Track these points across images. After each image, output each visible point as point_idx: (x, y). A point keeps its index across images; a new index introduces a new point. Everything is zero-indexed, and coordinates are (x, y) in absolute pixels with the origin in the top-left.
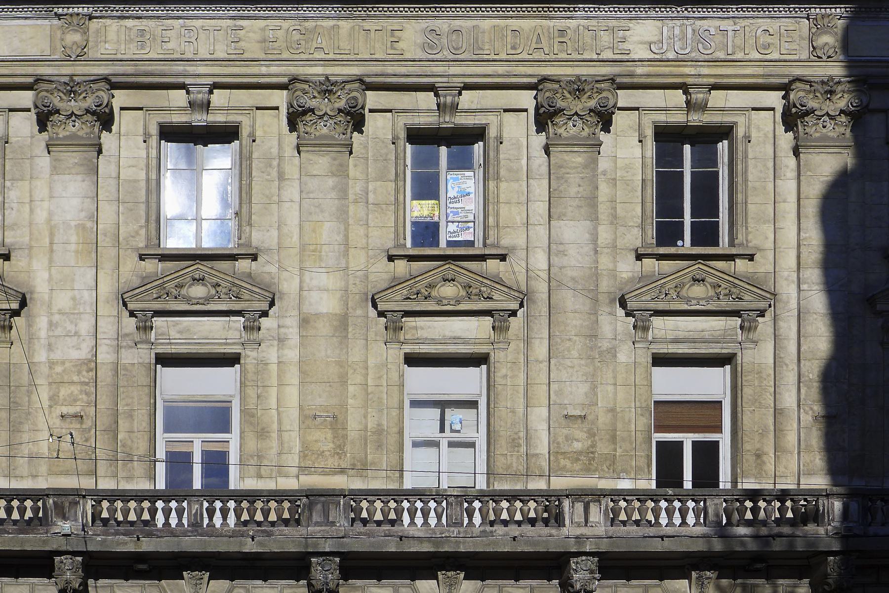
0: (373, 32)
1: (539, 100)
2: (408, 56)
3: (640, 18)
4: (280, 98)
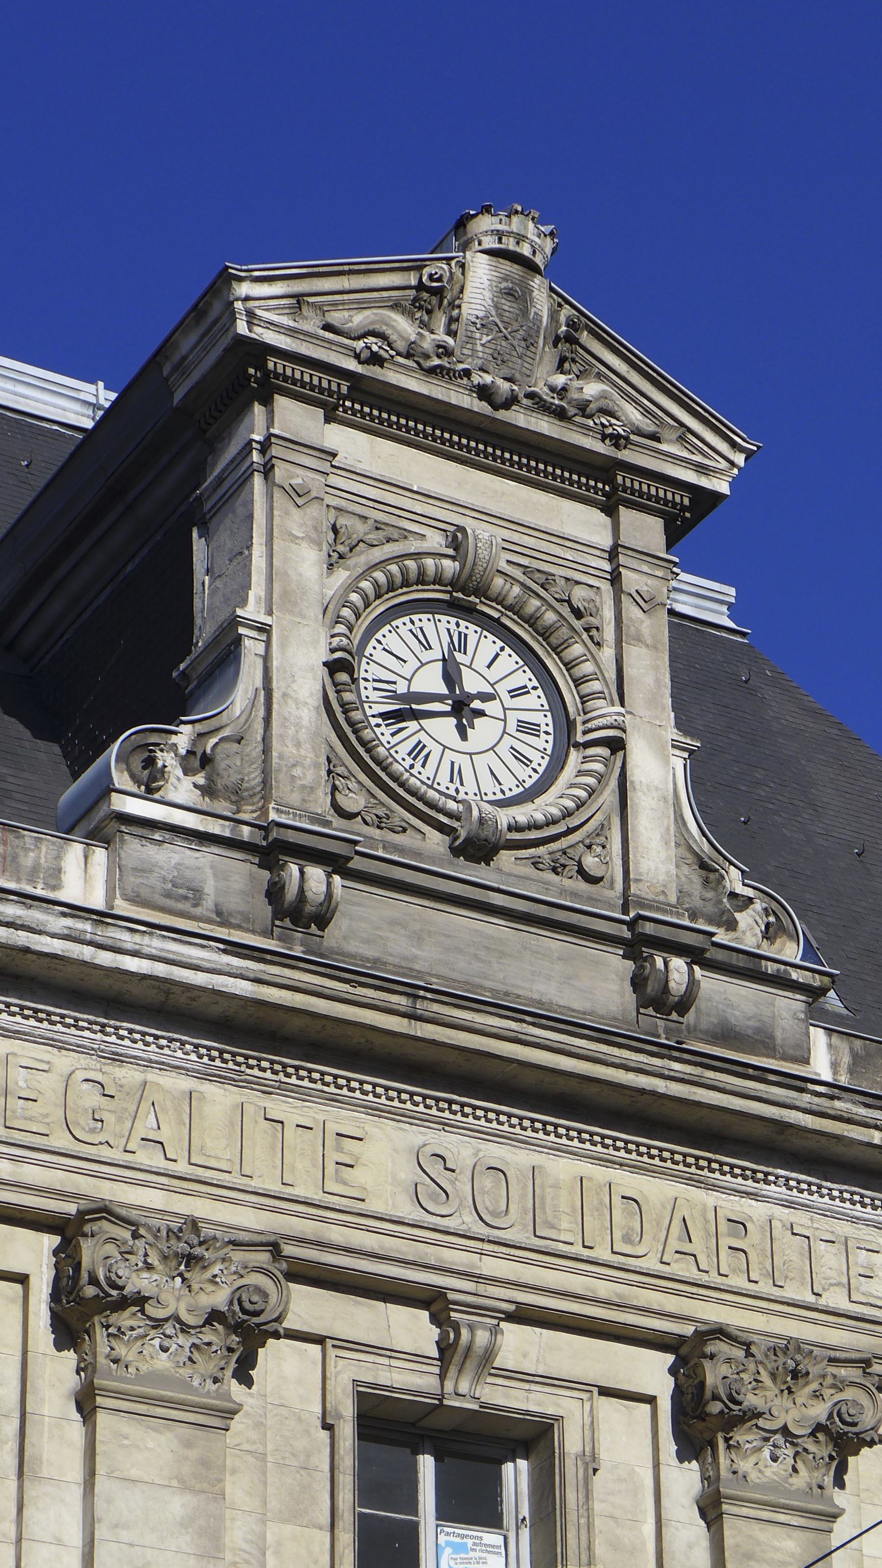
2: (375, 1206)
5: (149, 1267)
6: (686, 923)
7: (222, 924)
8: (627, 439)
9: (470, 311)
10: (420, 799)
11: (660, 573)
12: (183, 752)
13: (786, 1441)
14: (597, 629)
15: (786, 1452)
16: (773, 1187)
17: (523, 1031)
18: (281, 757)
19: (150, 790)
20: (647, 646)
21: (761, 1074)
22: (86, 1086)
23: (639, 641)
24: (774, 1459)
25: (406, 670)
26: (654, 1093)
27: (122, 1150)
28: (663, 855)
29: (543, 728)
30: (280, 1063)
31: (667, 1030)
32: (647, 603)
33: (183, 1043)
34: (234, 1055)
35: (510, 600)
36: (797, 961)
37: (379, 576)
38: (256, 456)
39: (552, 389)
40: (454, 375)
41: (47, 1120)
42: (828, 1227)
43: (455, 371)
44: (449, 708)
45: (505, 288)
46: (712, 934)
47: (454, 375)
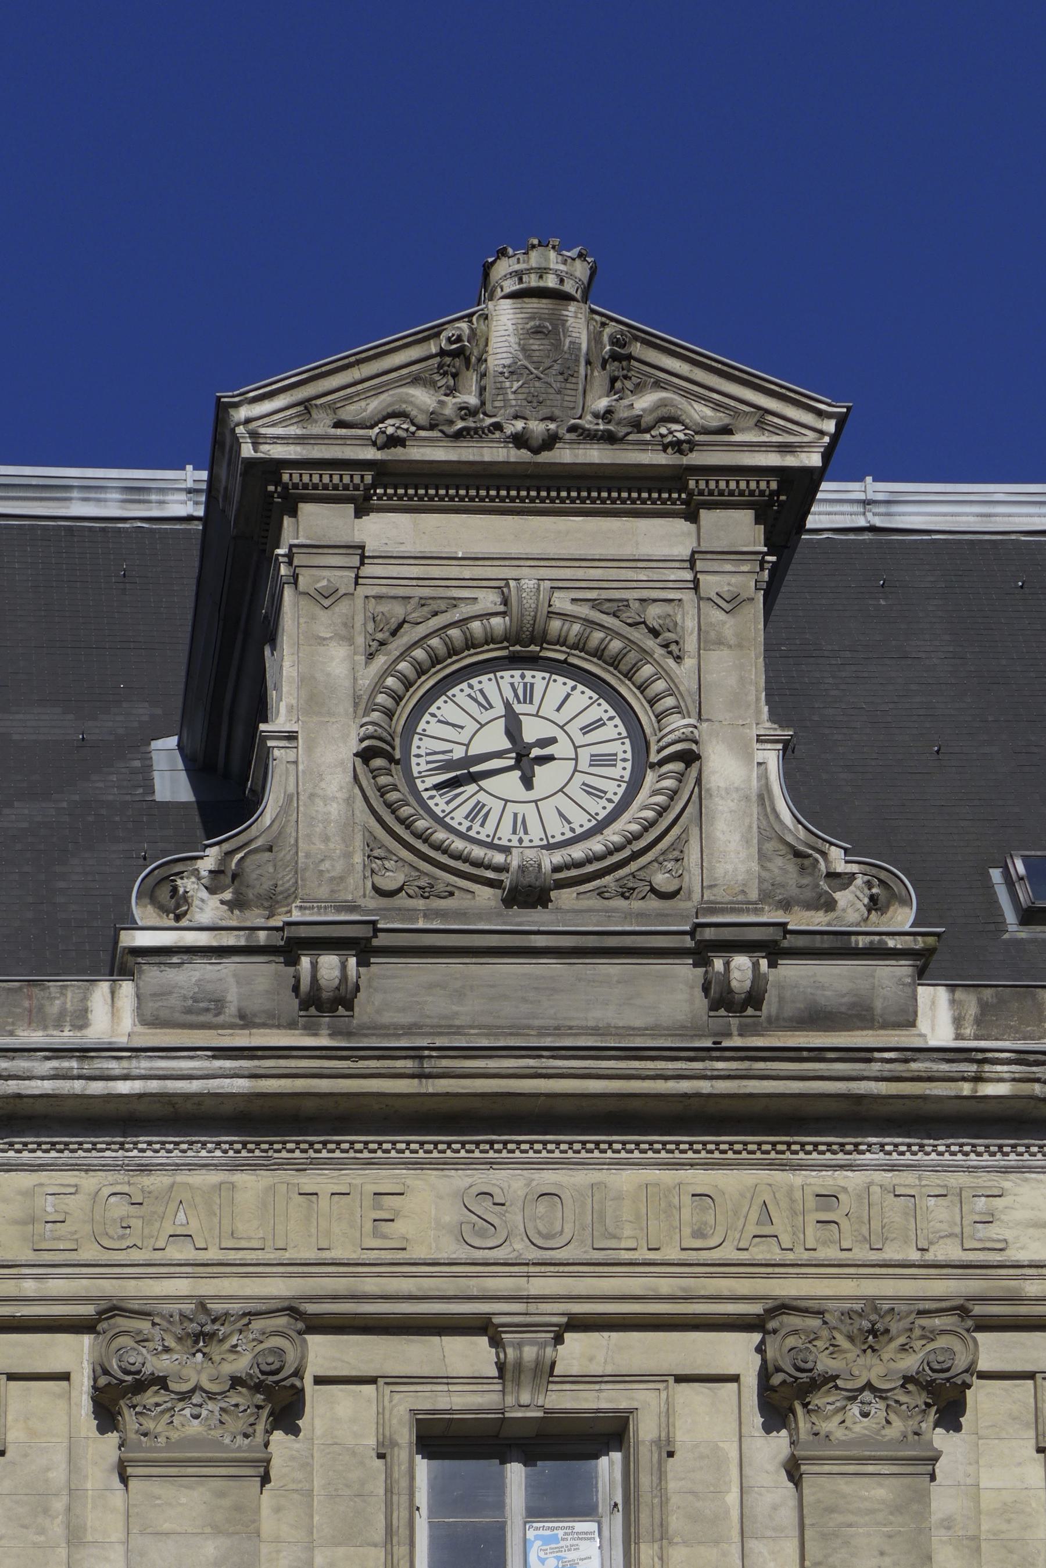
0: (324, 1202)
1: (770, 1354)
3: (1031, 1169)
4: (75, 1353)
9: (496, 362)
10: (466, 860)
11: (745, 568)
13: (875, 1397)
14: (677, 643)
15: (877, 1406)
16: (868, 1155)
18: (308, 856)
19: (178, 918)
22: (113, 1199)
23: (723, 644)
24: (865, 1415)
25: (464, 737)
28: (743, 855)
30: (305, 1142)
33: (204, 1144)
35: (572, 639)
37: (419, 654)
40: (483, 433)
41: (75, 1237)
42: (938, 1182)
43: (483, 429)
44: (512, 762)
45: (532, 328)
47: (483, 433)
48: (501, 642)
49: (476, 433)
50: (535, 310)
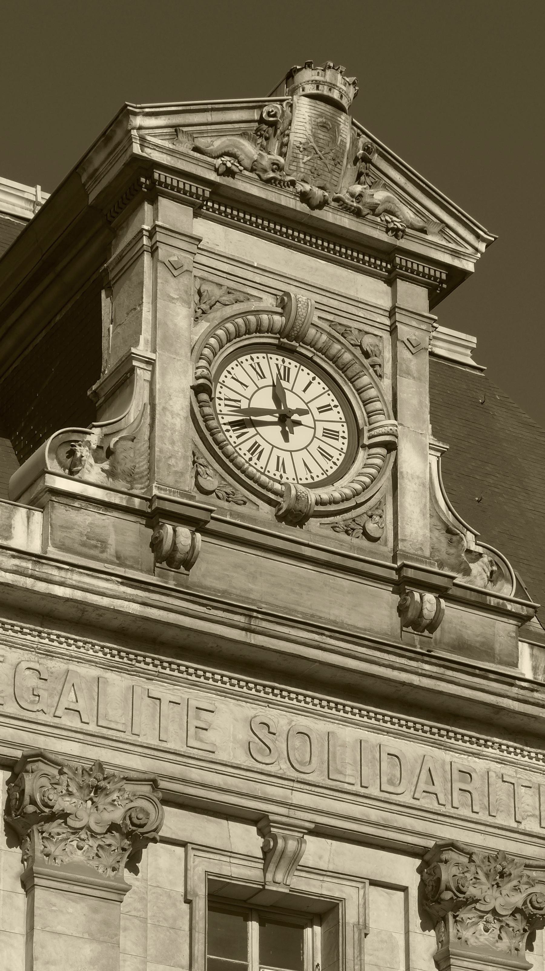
5: (70, 794)
6: (436, 570)
7: (120, 565)
8: (403, 231)
9: (296, 139)
10: (256, 481)
12: (94, 446)
17: (323, 641)
19: (72, 473)
20: (414, 378)
21: (484, 674)
22: (28, 672)
23: (409, 374)
26: (411, 685)
27: (52, 715)
28: (421, 523)
29: (341, 434)
30: (158, 659)
31: (421, 643)
32: (415, 348)
34: (128, 653)
35: (320, 345)
36: (512, 597)
37: (230, 326)
38: (145, 241)
39: (352, 195)
40: (284, 185)
43: (284, 182)
44: (276, 419)
45: (320, 122)
46: (453, 578)
47: (284, 185)
48: (276, 334)
49: (279, 183)
50: (323, 111)
